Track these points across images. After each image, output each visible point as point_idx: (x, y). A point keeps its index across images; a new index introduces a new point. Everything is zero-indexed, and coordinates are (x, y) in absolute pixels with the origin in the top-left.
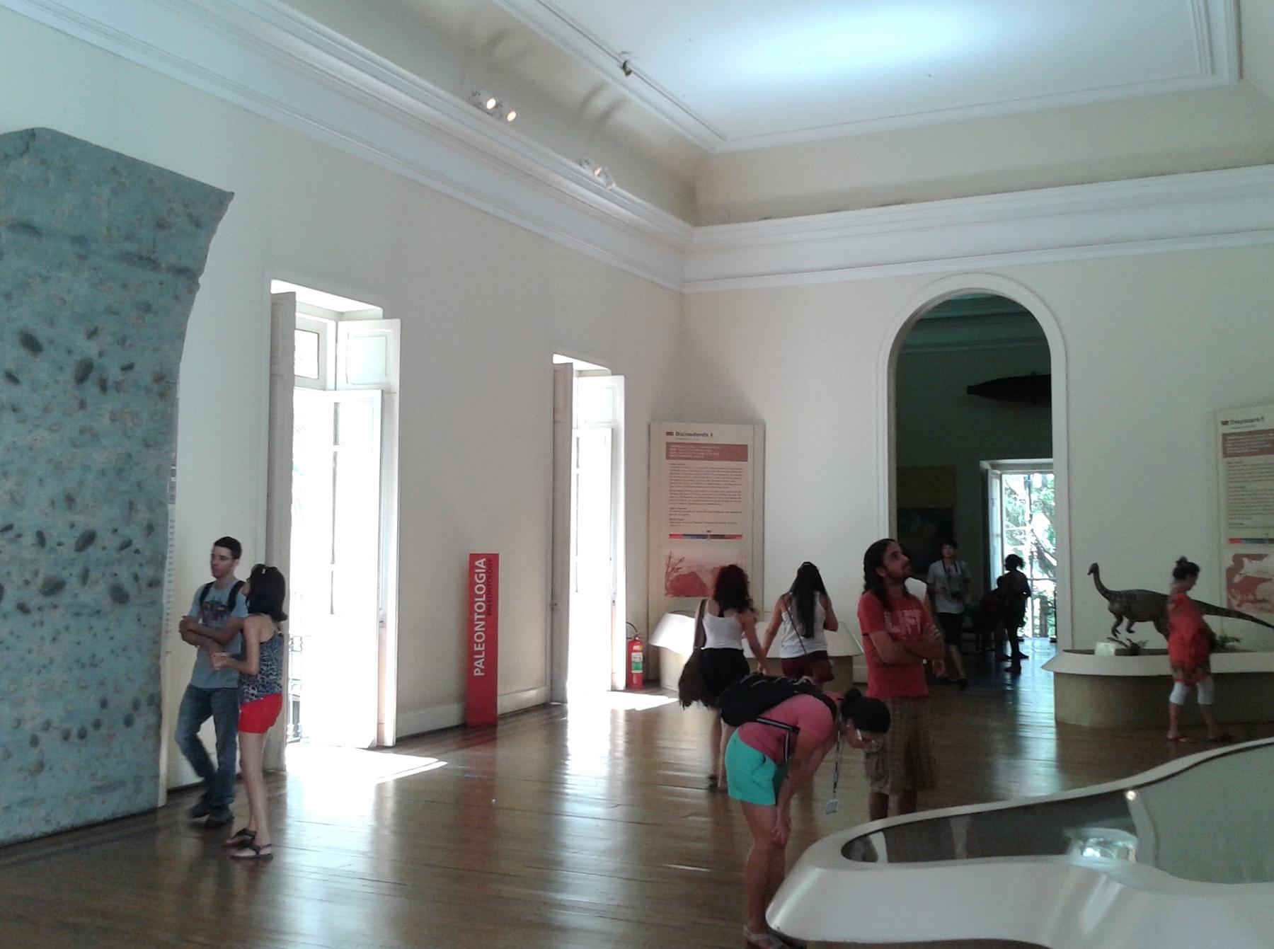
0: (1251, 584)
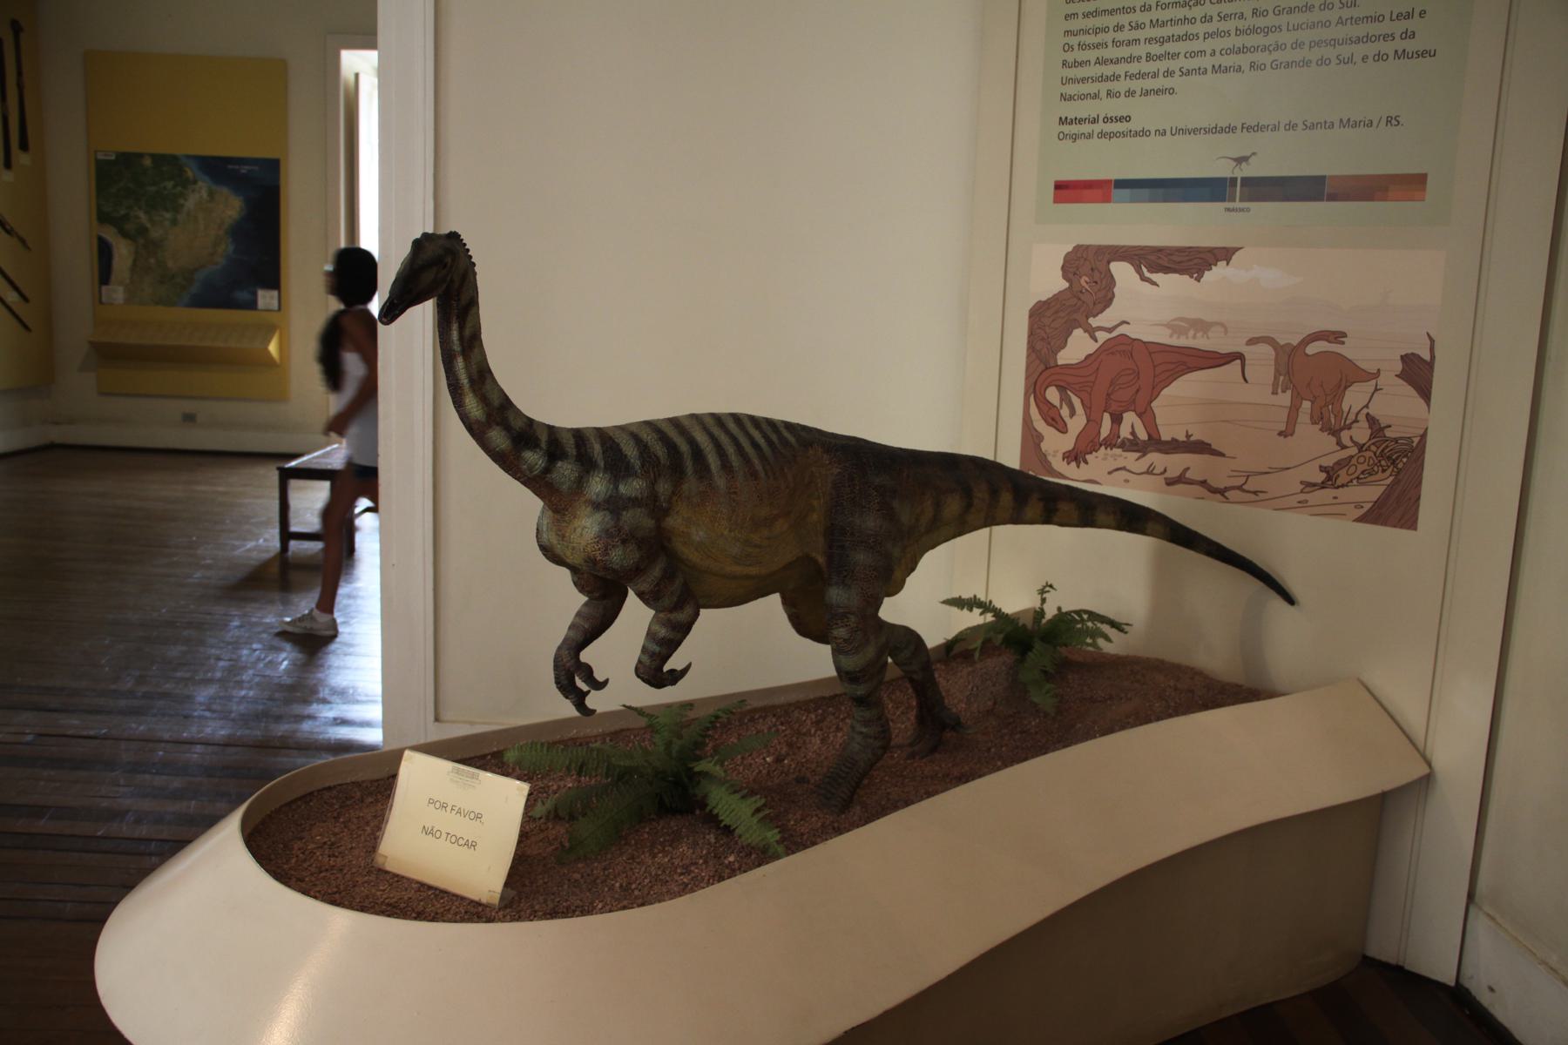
0: (1136, 371)
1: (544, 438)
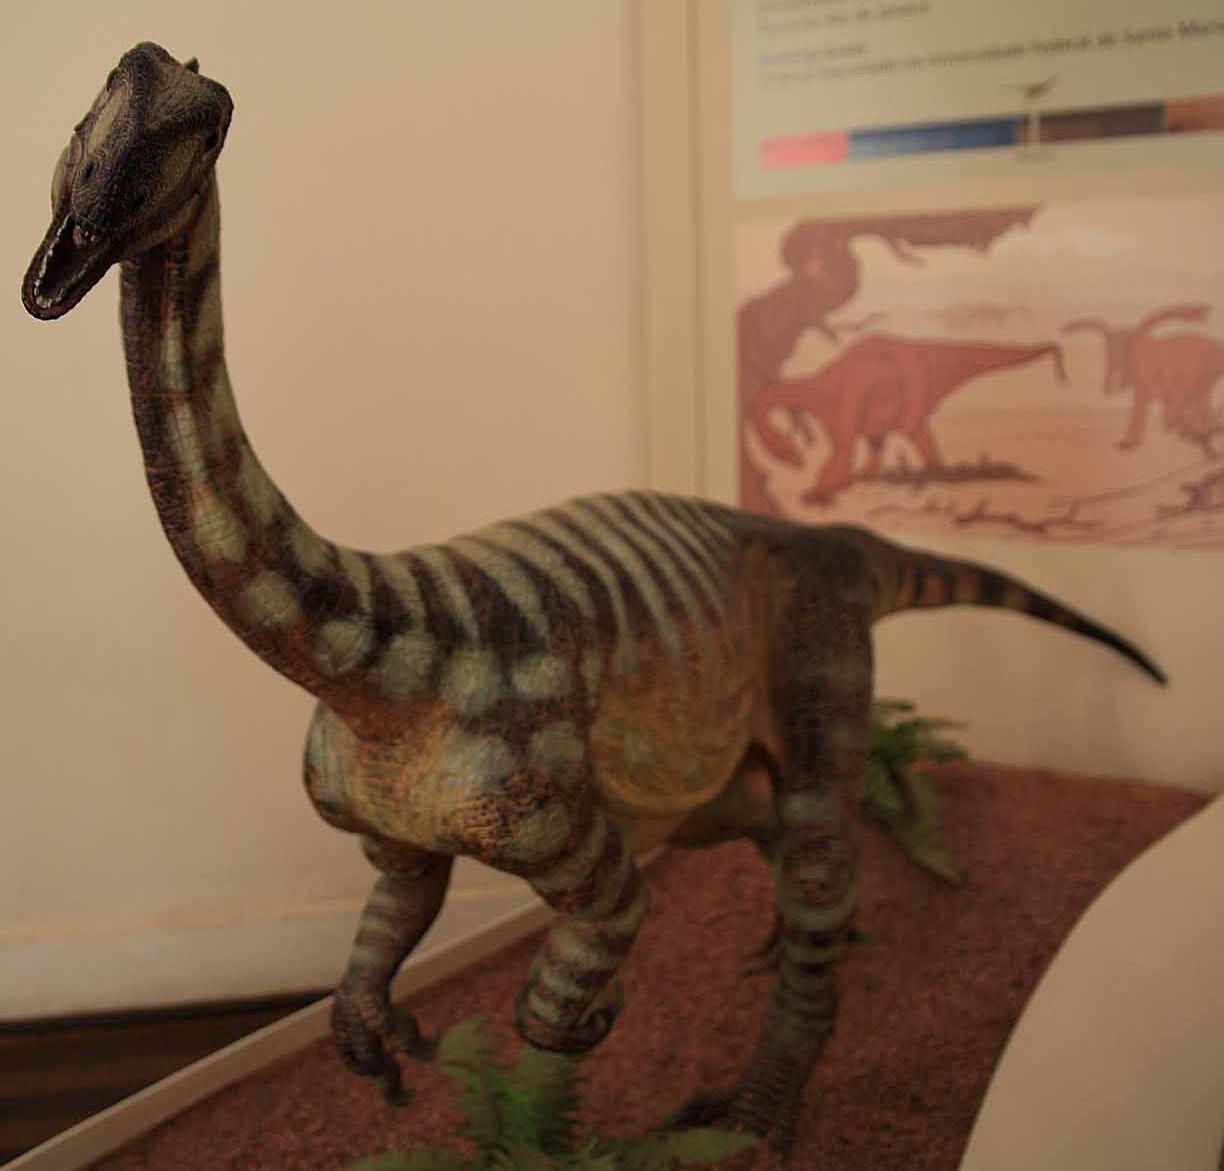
0: (906, 381)
1: (363, 586)
